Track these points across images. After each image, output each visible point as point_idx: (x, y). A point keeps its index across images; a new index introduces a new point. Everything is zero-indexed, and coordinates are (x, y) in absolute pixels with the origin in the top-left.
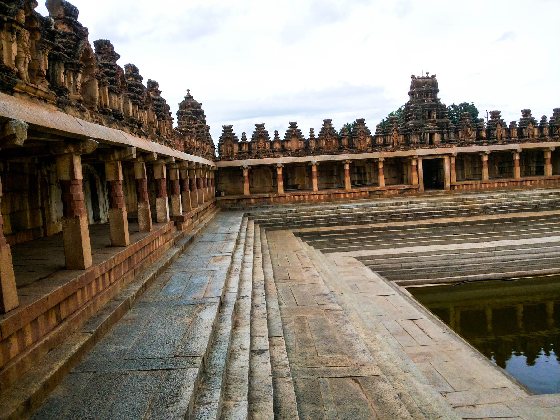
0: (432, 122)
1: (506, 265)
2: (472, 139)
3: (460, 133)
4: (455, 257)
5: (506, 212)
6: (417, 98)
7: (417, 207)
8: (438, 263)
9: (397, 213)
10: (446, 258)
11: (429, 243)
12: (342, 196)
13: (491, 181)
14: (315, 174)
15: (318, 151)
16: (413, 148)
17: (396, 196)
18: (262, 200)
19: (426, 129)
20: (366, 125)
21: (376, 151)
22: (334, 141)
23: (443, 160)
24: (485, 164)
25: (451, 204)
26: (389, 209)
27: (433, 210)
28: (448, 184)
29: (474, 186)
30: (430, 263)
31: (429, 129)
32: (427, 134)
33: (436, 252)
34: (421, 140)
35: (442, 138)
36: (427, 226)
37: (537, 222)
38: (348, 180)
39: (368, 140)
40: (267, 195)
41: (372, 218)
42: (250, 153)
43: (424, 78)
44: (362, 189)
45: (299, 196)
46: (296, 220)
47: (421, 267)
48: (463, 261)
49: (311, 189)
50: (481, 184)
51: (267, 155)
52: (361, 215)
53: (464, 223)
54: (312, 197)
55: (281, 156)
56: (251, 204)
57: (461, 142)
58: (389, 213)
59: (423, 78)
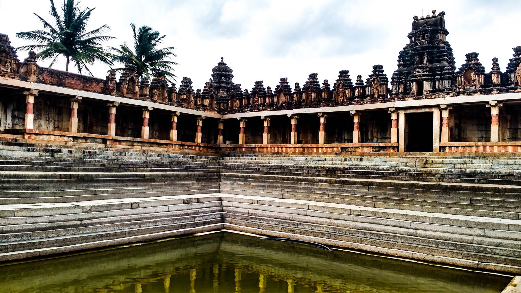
0: (420, 68)
1: (351, 234)
2: (475, 84)
3: (459, 78)
4: (305, 213)
5: (473, 182)
6: (413, 42)
7: (363, 164)
8: (281, 215)
9: (337, 168)
10: (296, 212)
11: (315, 198)
12: (315, 151)
13: (501, 143)
14: (293, 127)
15: (299, 105)
16: (394, 101)
17: (369, 154)
18: (250, 149)
19: (412, 77)
20: (350, 77)
21: (353, 104)
22: (313, 95)
23: (432, 113)
24: (494, 120)
25: (406, 166)
26: (333, 164)
27: (378, 169)
28: (436, 145)
29: (474, 149)
30: (273, 214)
31: (416, 77)
32: (413, 83)
33: (293, 204)
34: (405, 89)
35: (434, 87)
36: (336, 182)
37: (485, 195)
38: (322, 135)
39: (346, 92)
40: (253, 145)
41: (308, 171)
42: (247, 107)
43: (429, 18)
44: (334, 145)
45: (278, 147)
46: (249, 166)
47: (266, 217)
48: (308, 218)
49: (290, 143)
50: (484, 147)
52: (302, 167)
53: (380, 184)
54: (289, 150)
55: (269, 109)
56: (241, 152)
57: (457, 91)
58: (329, 168)
59: (427, 18)
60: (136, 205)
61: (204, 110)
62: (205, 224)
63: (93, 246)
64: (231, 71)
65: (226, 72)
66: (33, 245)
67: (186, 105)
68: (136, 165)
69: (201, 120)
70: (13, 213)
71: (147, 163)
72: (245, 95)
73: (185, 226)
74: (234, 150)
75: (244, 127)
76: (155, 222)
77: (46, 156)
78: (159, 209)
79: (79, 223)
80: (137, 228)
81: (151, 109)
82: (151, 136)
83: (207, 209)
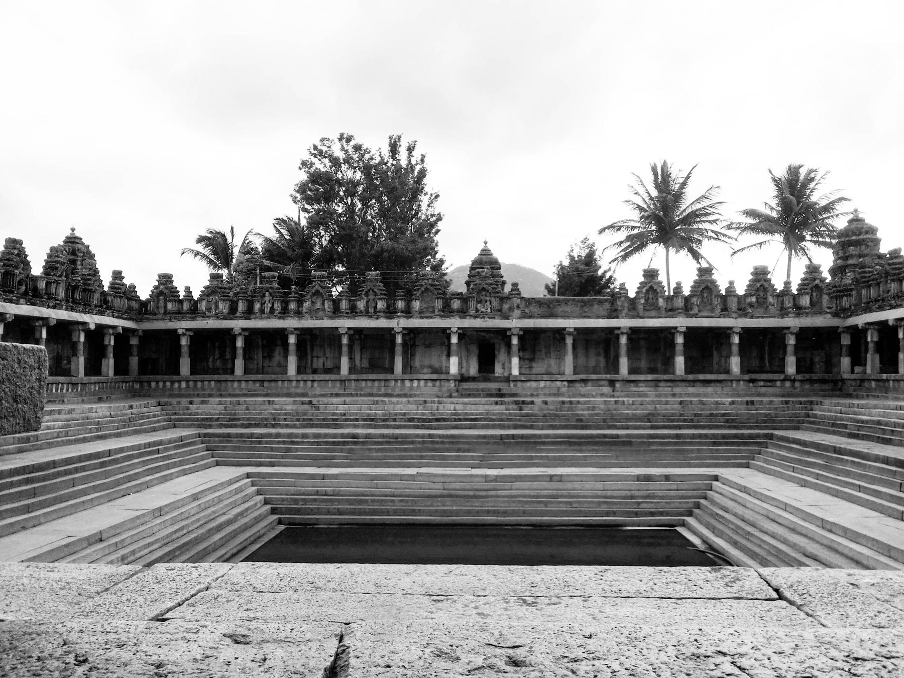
18: (881, 384)
42: (877, 301)
51: (890, 305)
56: (869, 389)
60: (558, 478)
61: (798, 315)
62: (652, 514)
63: (472, 522)
64: (872, 230)
65: (859, 235)
66: (413, 512)
67: (760, 311)
68: (628, 419)
69: (792, 333)
70: (412, 477)
71: (653, 415)
72: (873, 280)
73: (614, 514)
74: (860, 386)
75: (875, 339)
76: (570, 503)
77: (513, 410)
78: (599, 485)
79: (471, 493)
80: (541, 508)
81: (683, 329)
82: (689, 370)
83: (673, 493)
